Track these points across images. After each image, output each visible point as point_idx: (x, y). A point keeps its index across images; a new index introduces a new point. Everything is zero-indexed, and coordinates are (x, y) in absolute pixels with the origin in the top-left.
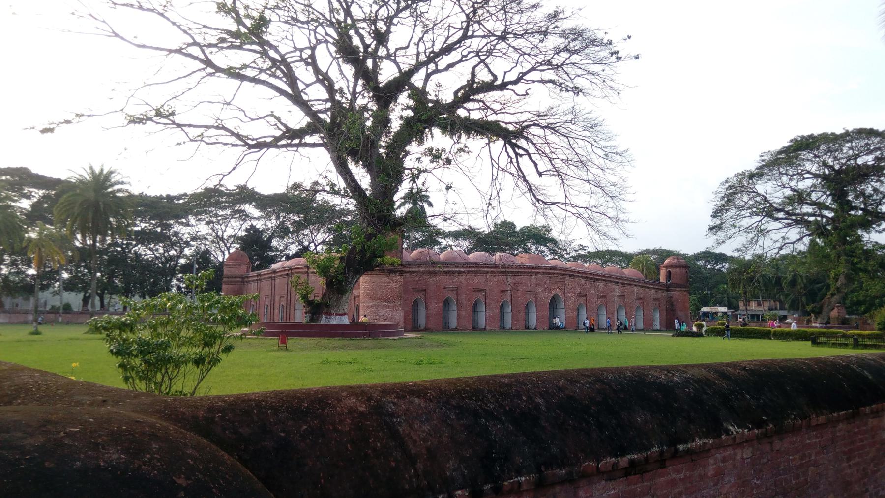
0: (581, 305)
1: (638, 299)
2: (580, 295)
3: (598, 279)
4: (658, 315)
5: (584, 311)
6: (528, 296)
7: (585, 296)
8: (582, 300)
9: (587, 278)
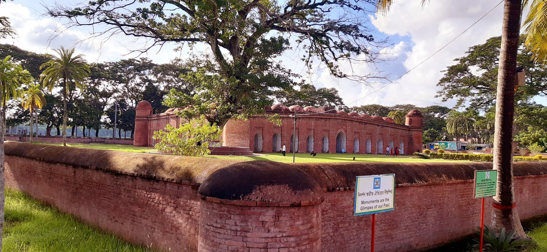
0: (356, 138)
1: (391, 135)
2: (355, 133)
5: (357, 143)
6: (324, 133)
7: (359, 133)
8: (356, 136)
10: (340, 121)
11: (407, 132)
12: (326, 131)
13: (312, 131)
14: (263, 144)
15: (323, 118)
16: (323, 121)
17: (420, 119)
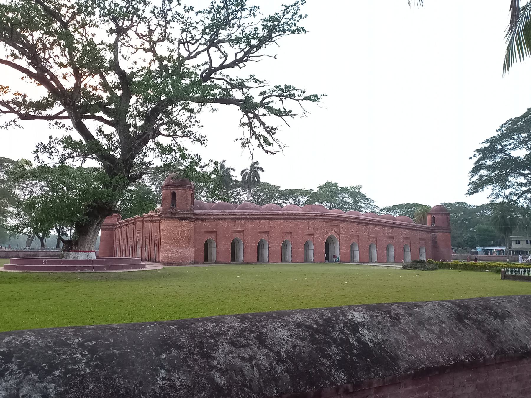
2: (353, 236)
3: (369, 224)
4: (425, 251)
6: (307, 237)
7: (358, 236)
8: (354, 240)
9: (359, 223)
12: (309, 234)
13: (289, 236)
14: (217, 253)
15: (304, 219)
16: (304, 223)
17: (445, 217)
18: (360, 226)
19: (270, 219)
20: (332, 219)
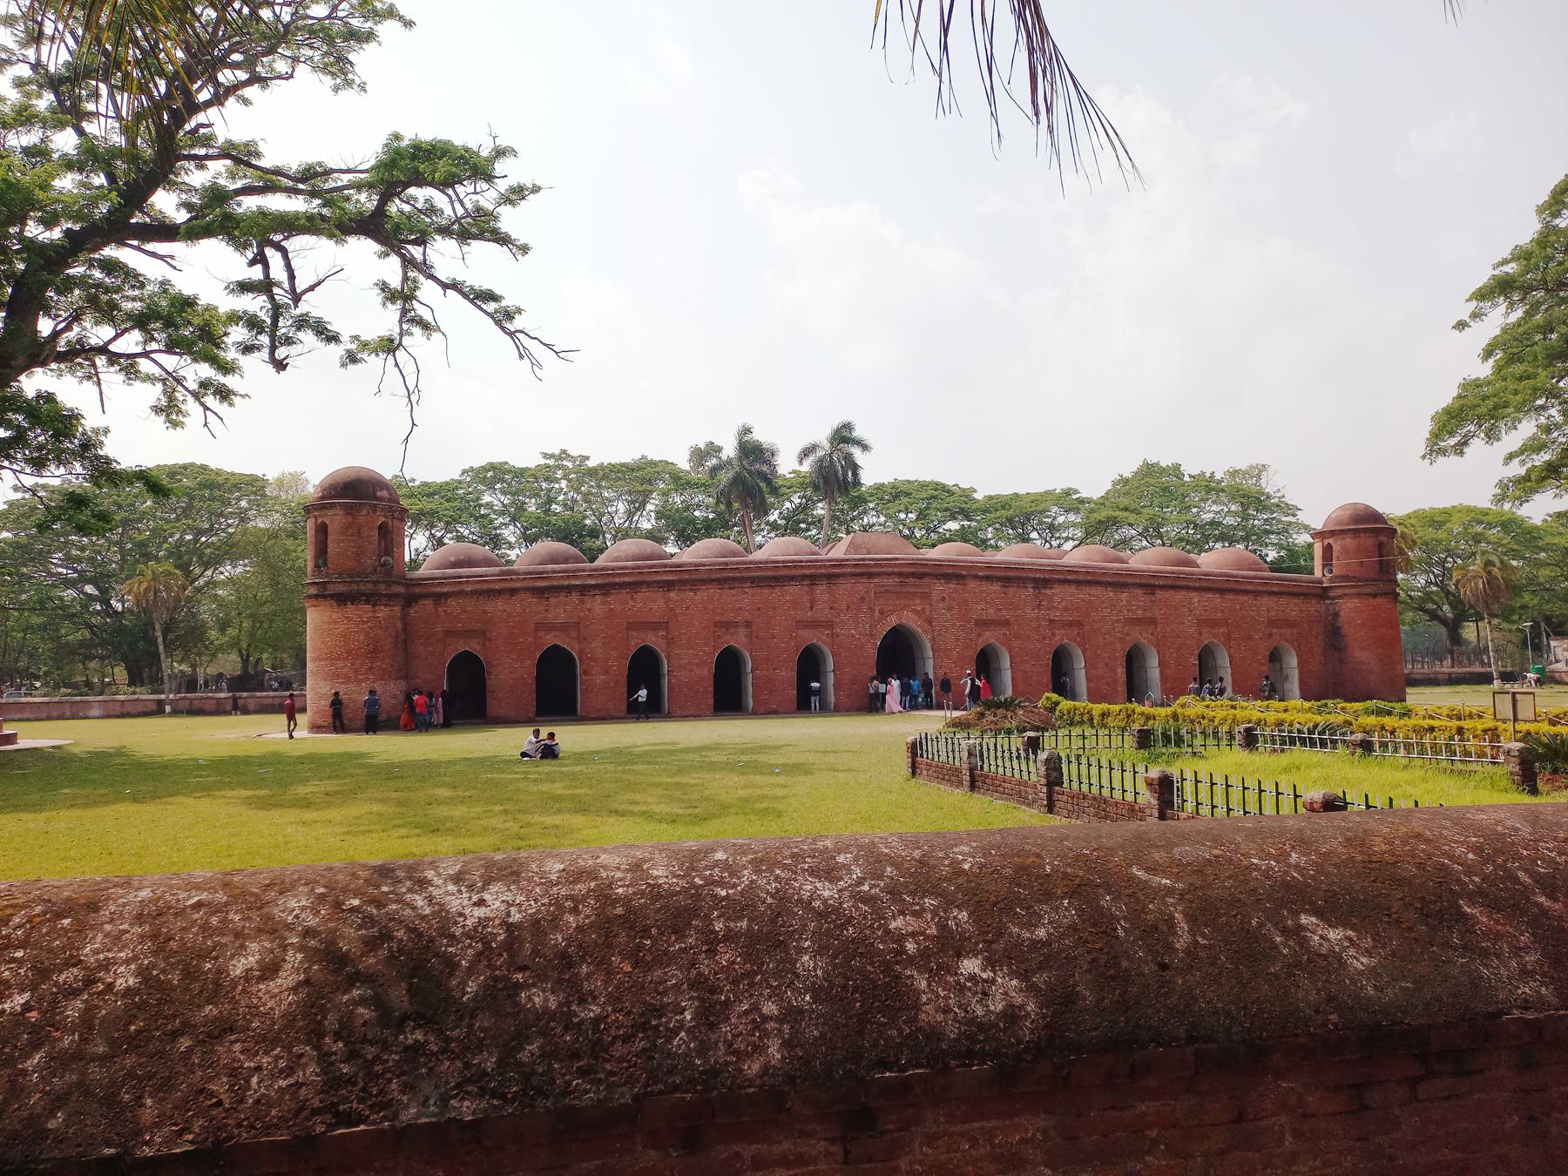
10: (889, 582)
11: (1313, 607)
18: (1011, 591)
19: (668, 585)
20: (900, 574)
